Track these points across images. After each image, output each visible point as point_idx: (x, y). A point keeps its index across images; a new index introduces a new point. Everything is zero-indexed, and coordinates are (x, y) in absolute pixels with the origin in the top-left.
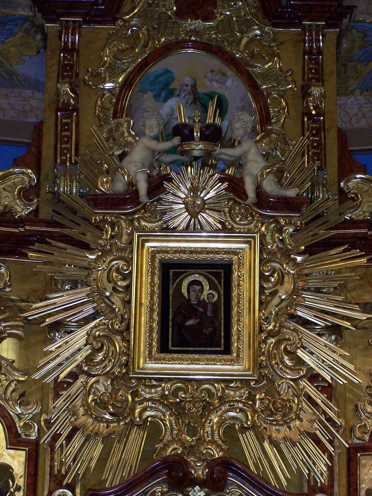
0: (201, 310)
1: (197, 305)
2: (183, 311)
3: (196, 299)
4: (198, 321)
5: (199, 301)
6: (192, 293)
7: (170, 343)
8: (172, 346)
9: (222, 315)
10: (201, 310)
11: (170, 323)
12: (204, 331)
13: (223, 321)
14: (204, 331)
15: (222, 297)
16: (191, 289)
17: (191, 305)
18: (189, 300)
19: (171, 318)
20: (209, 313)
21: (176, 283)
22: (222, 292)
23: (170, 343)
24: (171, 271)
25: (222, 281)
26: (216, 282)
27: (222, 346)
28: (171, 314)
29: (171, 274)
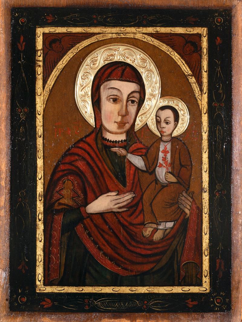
0: (138, 161)
1: (125, 145)
2: (81, 164)
3: (121, 125)
4: (127, 197)
5: (131, 132)
6: (107, 107)
7: (40, 270)
8: (46, 283)
9: (206, 177)
10: (138, 161)
11: (40, 207)
12: (147, 232)
13: (206, 196)
14: (147, 232)
15: (205, 119)
16: (104, 94)
17: (107, 146)
18: (99, 128)
19: (40, 189)
20: (162, 173)
21: (55, 73)
22: (204, 102)
23: (40, 270)
24: (40, 31)
25: (205, 64)
26: (186, 69)
27: (206, 280)
28: (40, 174)
29: (40, 44)
